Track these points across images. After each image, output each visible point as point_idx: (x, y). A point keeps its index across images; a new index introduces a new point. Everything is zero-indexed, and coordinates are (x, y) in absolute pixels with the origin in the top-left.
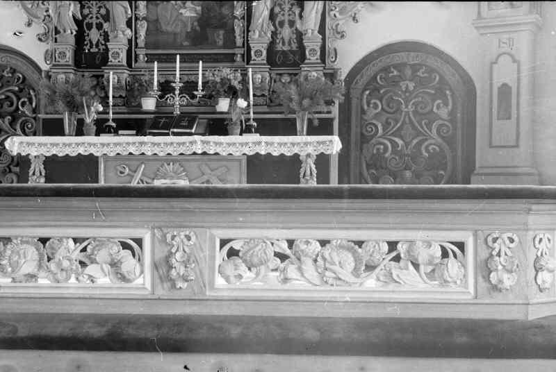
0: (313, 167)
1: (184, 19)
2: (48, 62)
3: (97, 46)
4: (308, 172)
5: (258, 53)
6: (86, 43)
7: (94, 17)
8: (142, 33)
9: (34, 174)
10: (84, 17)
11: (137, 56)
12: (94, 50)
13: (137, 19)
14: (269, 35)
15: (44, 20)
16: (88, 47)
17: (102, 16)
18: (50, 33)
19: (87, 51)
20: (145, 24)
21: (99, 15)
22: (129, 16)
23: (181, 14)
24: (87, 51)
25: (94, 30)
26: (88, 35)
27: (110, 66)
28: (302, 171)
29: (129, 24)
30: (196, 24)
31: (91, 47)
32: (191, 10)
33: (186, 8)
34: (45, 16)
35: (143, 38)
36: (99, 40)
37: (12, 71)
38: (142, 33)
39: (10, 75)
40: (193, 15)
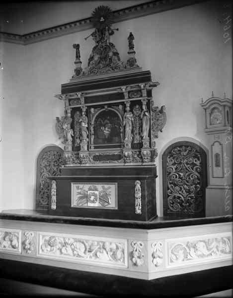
0: (140, 187)
4: (138, 189)
8: (92, 139)
11: (91, 147)
13: (90, 135)
14: (131, 138)
20: (93, 136)
28: (136, 188)
29: (88, 137)
32: (108, 131)
38: (92, 139)
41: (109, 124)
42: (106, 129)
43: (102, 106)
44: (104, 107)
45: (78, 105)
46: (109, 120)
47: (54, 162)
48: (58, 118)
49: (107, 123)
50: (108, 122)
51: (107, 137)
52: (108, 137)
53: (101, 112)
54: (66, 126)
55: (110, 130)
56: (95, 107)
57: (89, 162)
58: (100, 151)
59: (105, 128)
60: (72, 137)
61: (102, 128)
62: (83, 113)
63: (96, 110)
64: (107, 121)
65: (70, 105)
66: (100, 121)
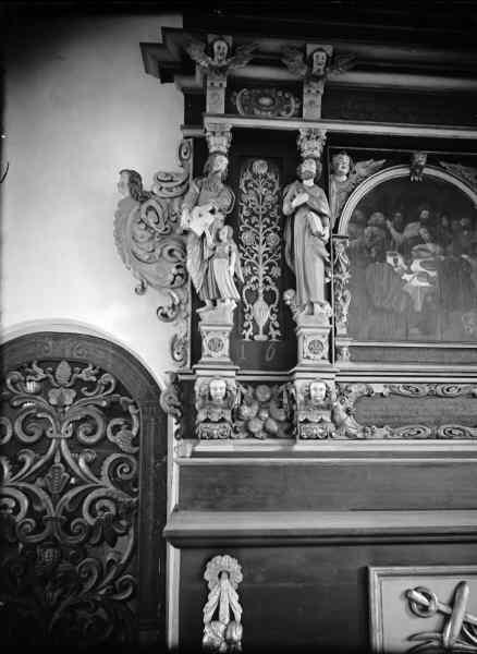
1: (410, 291)
2: (176, 356)
3: (266, 331)
5: (216, 345)
6: (246, 325)
7: (261, 281)
9: (216, 617)
10: (247, 278)
12: (261, 337)
15: (173, 283)
16: (250, 331)
17: (274, 279)
18: (182, 307)
19: (247, 339)
21: (268, 279)
22: (328, 281)
23: (406, 281)
24: (247, 339)
25: (261, 304)
26: (249, 312)
27: (203, 363)
30: (429, 299)
31: (256, 333)
32: (421, 275)
33: (410, 272)
34: (175, 276)
35: (345, 319)
36: (269, 320)
37: (96, 371)
39: (94, 379)
40: (424, 284)
41: (430, 246)
42: (416, 266)
43: (394, 152)
44: (406, 160)
45: (278, 117)
46: (425, 224)
47: (77, 423)
48: (134, 178)
49: (418, 240)
50: (423, 232)
51: (419, 308)
52: (425, 304)
53: (379, 188)
54: (210, 219)
55: (433, 274)
56: (361, 148)
57: (331, 427)
58: (403, 374)
59: (408, 262)
60: (239, 286)
61: (390, 260)
62: (310, 167)
63: (361, 168)
64: (412, 229)
65: (230, 111)
66: (383, 227)
